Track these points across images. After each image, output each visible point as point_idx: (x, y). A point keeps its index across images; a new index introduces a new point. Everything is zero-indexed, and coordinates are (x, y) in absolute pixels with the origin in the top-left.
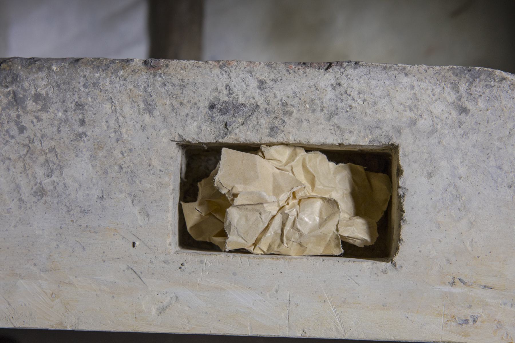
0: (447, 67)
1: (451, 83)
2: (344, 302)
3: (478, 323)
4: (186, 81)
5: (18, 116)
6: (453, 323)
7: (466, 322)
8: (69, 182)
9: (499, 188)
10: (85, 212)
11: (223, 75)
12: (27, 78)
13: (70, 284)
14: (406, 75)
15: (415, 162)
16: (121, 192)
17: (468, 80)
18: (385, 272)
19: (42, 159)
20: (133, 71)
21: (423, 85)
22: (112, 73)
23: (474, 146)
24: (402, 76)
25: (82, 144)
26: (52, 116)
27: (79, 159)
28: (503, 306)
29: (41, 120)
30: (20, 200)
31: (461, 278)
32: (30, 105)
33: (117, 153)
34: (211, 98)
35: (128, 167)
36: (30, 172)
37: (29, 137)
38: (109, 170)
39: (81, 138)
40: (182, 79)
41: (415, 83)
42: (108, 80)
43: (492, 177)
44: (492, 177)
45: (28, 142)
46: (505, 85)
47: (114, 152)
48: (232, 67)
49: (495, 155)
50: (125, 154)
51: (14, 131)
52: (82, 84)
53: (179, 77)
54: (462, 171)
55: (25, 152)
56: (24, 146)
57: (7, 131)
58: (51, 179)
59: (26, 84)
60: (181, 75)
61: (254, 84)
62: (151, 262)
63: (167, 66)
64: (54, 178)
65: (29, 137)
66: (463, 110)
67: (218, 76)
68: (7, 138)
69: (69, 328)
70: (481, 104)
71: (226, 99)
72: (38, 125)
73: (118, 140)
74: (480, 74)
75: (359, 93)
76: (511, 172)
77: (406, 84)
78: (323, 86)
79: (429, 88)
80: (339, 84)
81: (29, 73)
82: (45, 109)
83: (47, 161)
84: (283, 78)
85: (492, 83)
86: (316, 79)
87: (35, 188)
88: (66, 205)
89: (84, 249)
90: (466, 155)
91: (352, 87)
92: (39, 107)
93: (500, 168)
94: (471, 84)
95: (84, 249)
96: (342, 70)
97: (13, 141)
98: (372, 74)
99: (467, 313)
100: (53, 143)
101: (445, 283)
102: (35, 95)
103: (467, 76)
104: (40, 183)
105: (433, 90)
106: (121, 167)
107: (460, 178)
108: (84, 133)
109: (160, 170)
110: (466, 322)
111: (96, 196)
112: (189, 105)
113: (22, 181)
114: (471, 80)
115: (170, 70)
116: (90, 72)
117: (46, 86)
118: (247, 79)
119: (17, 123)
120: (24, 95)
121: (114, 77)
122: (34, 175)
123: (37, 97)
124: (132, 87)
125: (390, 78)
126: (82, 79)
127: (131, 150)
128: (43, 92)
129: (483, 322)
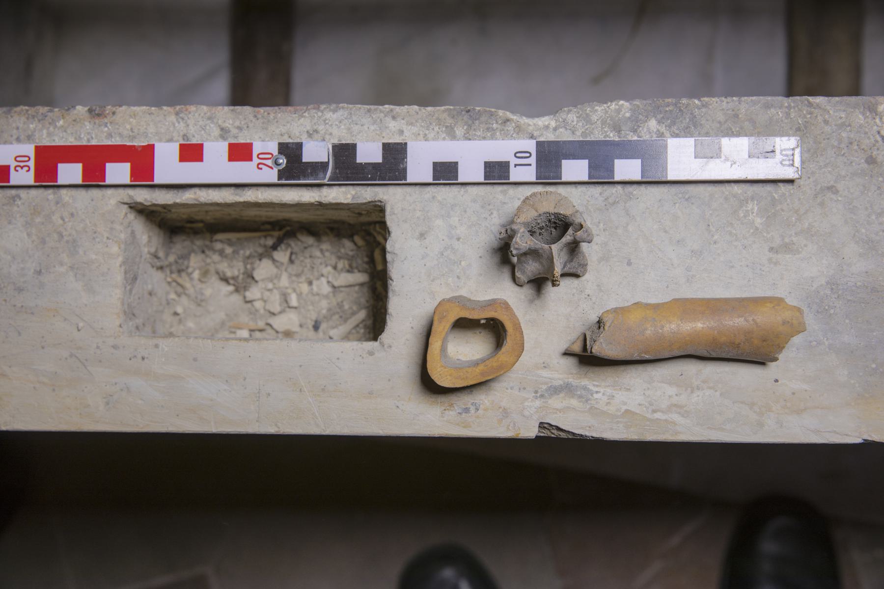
0: (443, 108)
1: (447, 127)
2: (323, 390)
4: (136, 131)
6: (451, 413)
10: (20, 290)
11: (179, 123)
14: (394, 118)
15: (405, 221)
16: (61, 264)
17: (466, 123)
18: (371, 353)
20: (74, 121)
21: (415, 129)
22: (50, 123)
23: (474, 201)
24: (388, 119)
25: (16, 208)
27: (11, 227)
28: (509, 391)
33: (56, 218)
35: (70, 235)
38: (47, 239)
39: (14, 201)
40: (132, 129)
41: (404, 128)
42: (45, 132)
46: (510, 127)
47: (53, 218)
48: (190, 113)
49: (498, 210)
50: (66, 220)
52: (15, 137)
53: (128, 127)
54: (461, 231)
60: (130, 123)
62: (98, 347)
63: (114, 113)
67: (174, 124)
73: (57, 203)
77: (394, 129)
78: (298, 134)
79: (421, 133)
80: (316, 131)
84: (251, 125)
85: (495, 126)
86: (289, 125)
89: (20, 334)
90: (465, 211)
91: (331, 134)
94: (470, 126)
95: (20, 334)
96: (320, 114)
98: (354, 118)
103: (465, 118)
105: (426, 135)
106: (61, 236)
107: (458, 239)
109: (108, 238)
111: (32, 271)
114: (470, 122)
115: (118, 118)
116: (24, 123)
118: (208, 127)
121: (51, 129)
125: (374, 123)
126: (15, 131)
127: (72, 215)
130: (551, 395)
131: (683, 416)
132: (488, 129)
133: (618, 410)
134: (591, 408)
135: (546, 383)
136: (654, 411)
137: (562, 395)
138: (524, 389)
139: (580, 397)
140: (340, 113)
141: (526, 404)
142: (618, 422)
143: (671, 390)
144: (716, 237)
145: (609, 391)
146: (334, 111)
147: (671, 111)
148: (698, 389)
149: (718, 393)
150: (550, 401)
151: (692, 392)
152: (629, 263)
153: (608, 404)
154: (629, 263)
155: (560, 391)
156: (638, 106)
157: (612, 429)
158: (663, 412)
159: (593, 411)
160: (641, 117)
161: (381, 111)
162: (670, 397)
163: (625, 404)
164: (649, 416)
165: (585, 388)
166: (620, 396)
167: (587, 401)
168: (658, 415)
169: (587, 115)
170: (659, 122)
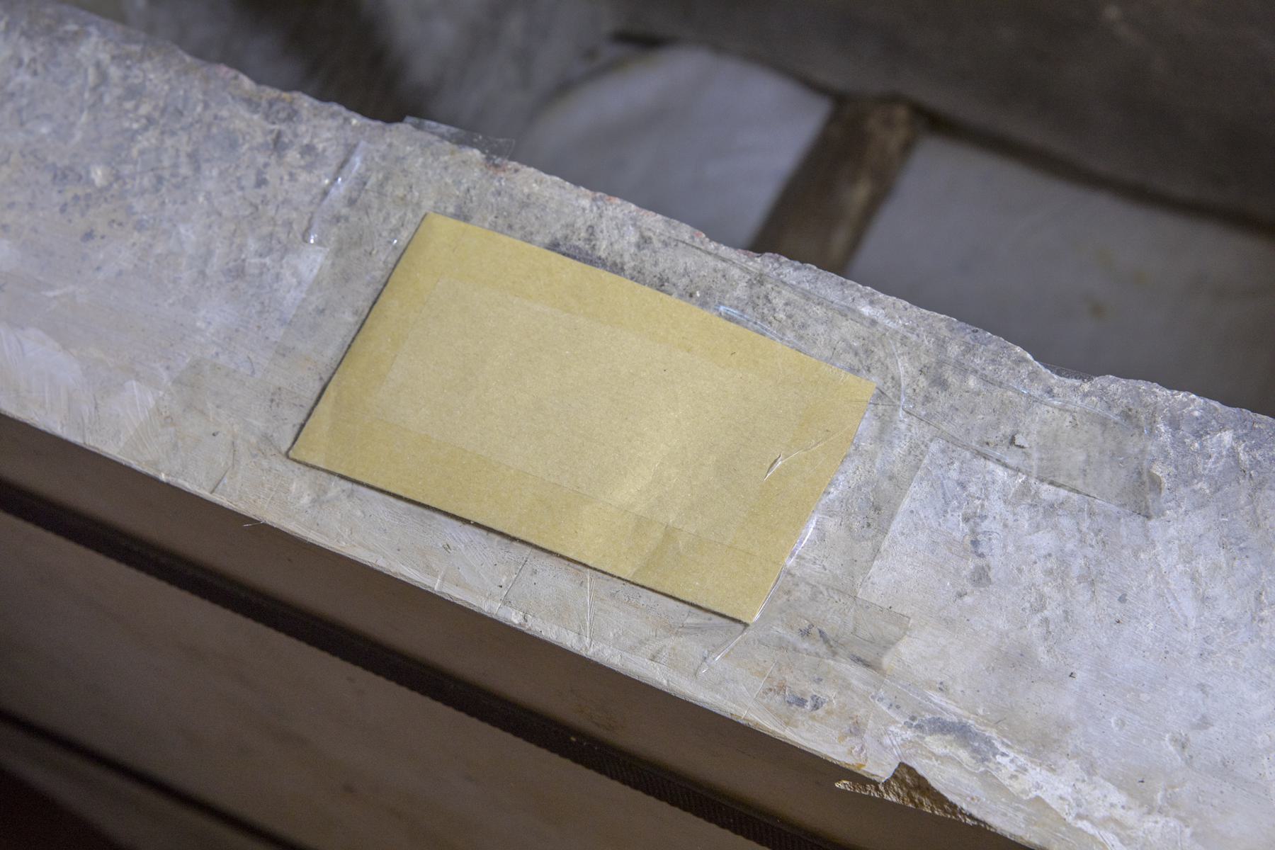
1: (938, 339)
3: (820, 712)
4: (533, 199)
5: (266, 165)
7: (801, 702)
8: (287, 273)
9: (949, 516)
12: (308, 120)
13: (202, 412)
14: (872, 303)
19: (266, 230)
26: (315, 180)
29: (296, 180)
30: (202, 273)
31: (824, 629)
32: (293, 156)
34: (559, 235)
36: (238, 241)
37: (264, 196)
42: (421, 160)
43: (944, 494)
44: (944, 494)
45: (258, 201)
46: (1024, 371)
49: (962, 462)
51: (249, 181)
55: (247, 213)
56: (251, 204)
57: (239, 179)
58: (263, 261)
59: (302, 128)
61: (633, 237)
63: (516, 171)
64: (267, 260)
65: (264, 196)
66: (942, 384)
68: (234, 187)
69: (163, 477)
70: (972, 382)
71: (581, 244)
72: (287, 185)
74: (990, 342)
75: (786, 304)
76: (978, 498)
81: (315, 115)
82: (309, 168)
83: (271, 235)
87: (232, 264)
88: (262, 303)
92: (302, 163)
93: (963, 485)
96: (776, 265)
97: (239, 193)
99: (812, 689)
100: (294, 215)
101: (792, 628)
102: (307, 146)
103: (968, 337)
104: (244, 261)
108: (347, 219)
110: (801, 702)
112: (521, 232)
113: (220, 249)
115: (519, 178)
117: (328, 140)
119: (259, 173)
120: (291, 142)
121: (430, 160)
122: (241, 248)
123: (308, 149)
124: (449, 181)
128: (320, 147)
129: (829, 713)
130: (933, 732)
131: (1122, 841)
132: (993, 360)
133: (1024, 791)
134: (986, 772)
135: (933, 712)
136: (1079, 817)
137: (949, 737)
138: (898, 707)
139: (976, 750)
140: (805, 273)
141: (892, 728)
142: (1017, 809)
143: (1117, 797)
144: (1265, 613)
145: (1022, 760)
146: (796, 269)
147: (1260, 430)
148: (1160, 812)
149: (1188, 831)
150: (928, 739)
151: (1149, 813)
152: (1122, 599)
153: (1013, 777)
154: (1122, 599)
155: (949, 732)
156: (1216, 409)
157: (1005, 815)
158: (1092, 822)
159: (989, 780)
160: (1214, 422)
161: (858, 290)
162: (1112, 805)
163: (1038, 787)
164: (1070, 819)
165: (988, 741)
166: (1036, 774)
167: (984, 760)
168: (1084, 825)
169: (1139, 394)
170: (1238, 438)
